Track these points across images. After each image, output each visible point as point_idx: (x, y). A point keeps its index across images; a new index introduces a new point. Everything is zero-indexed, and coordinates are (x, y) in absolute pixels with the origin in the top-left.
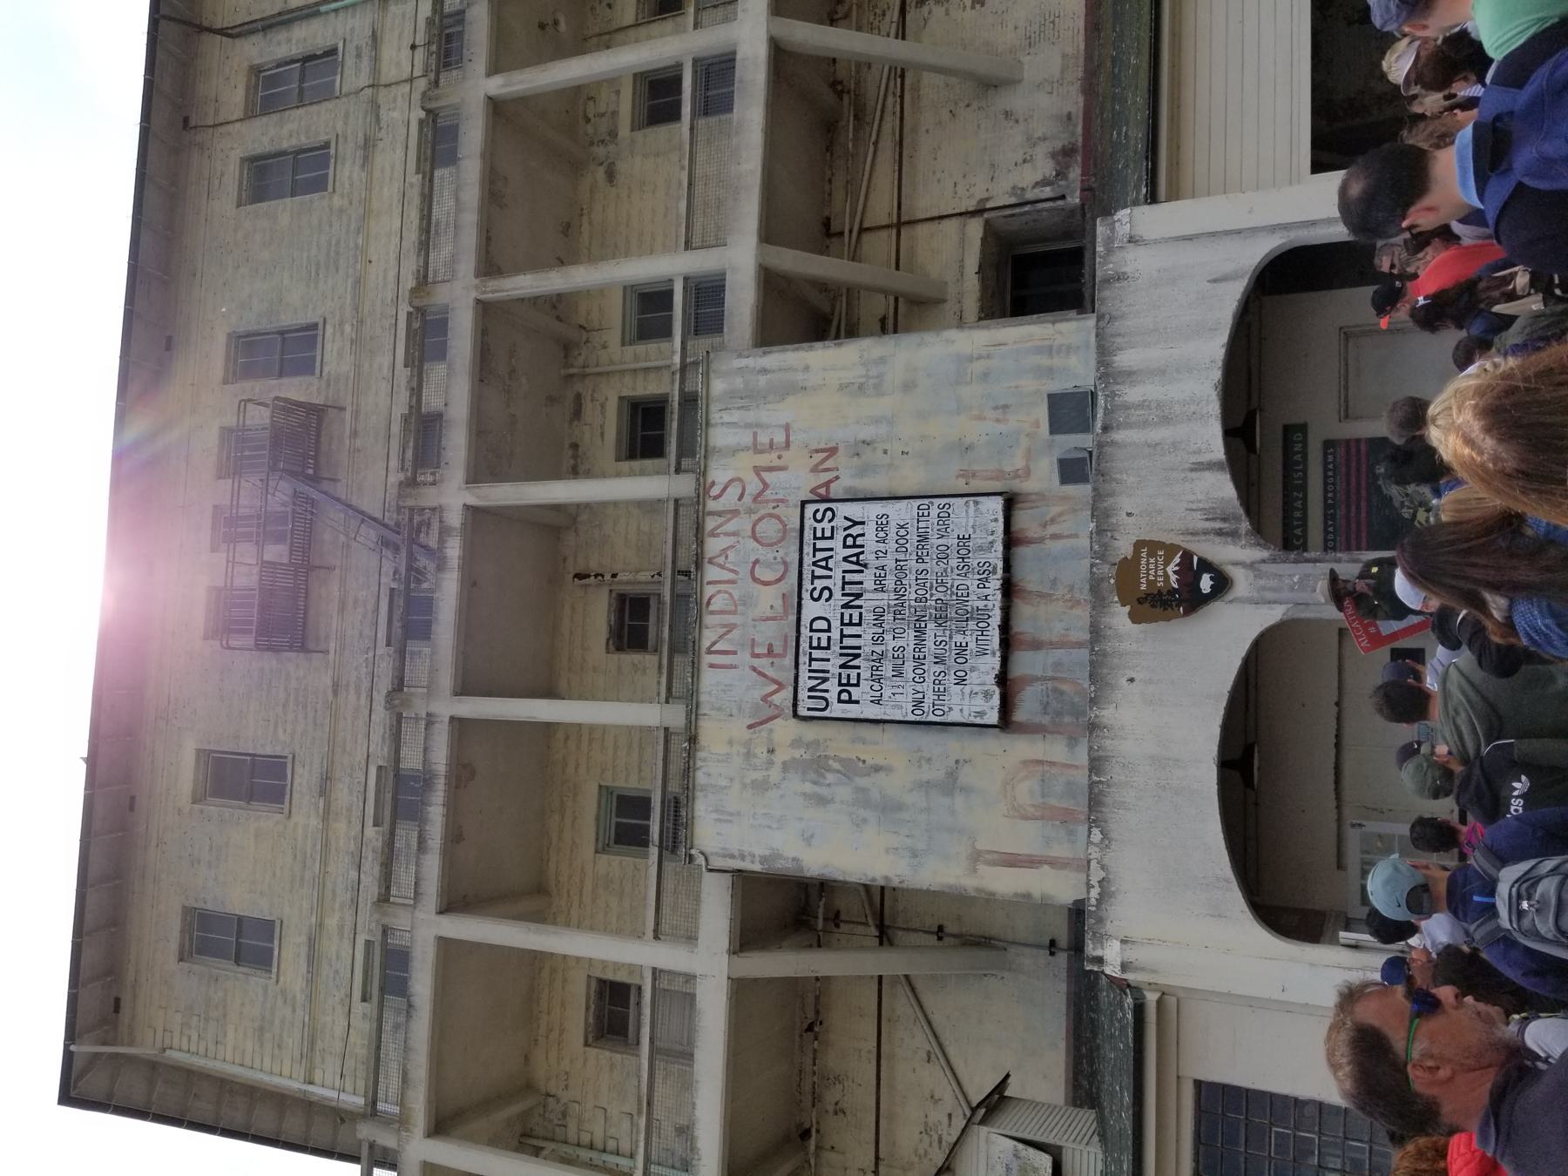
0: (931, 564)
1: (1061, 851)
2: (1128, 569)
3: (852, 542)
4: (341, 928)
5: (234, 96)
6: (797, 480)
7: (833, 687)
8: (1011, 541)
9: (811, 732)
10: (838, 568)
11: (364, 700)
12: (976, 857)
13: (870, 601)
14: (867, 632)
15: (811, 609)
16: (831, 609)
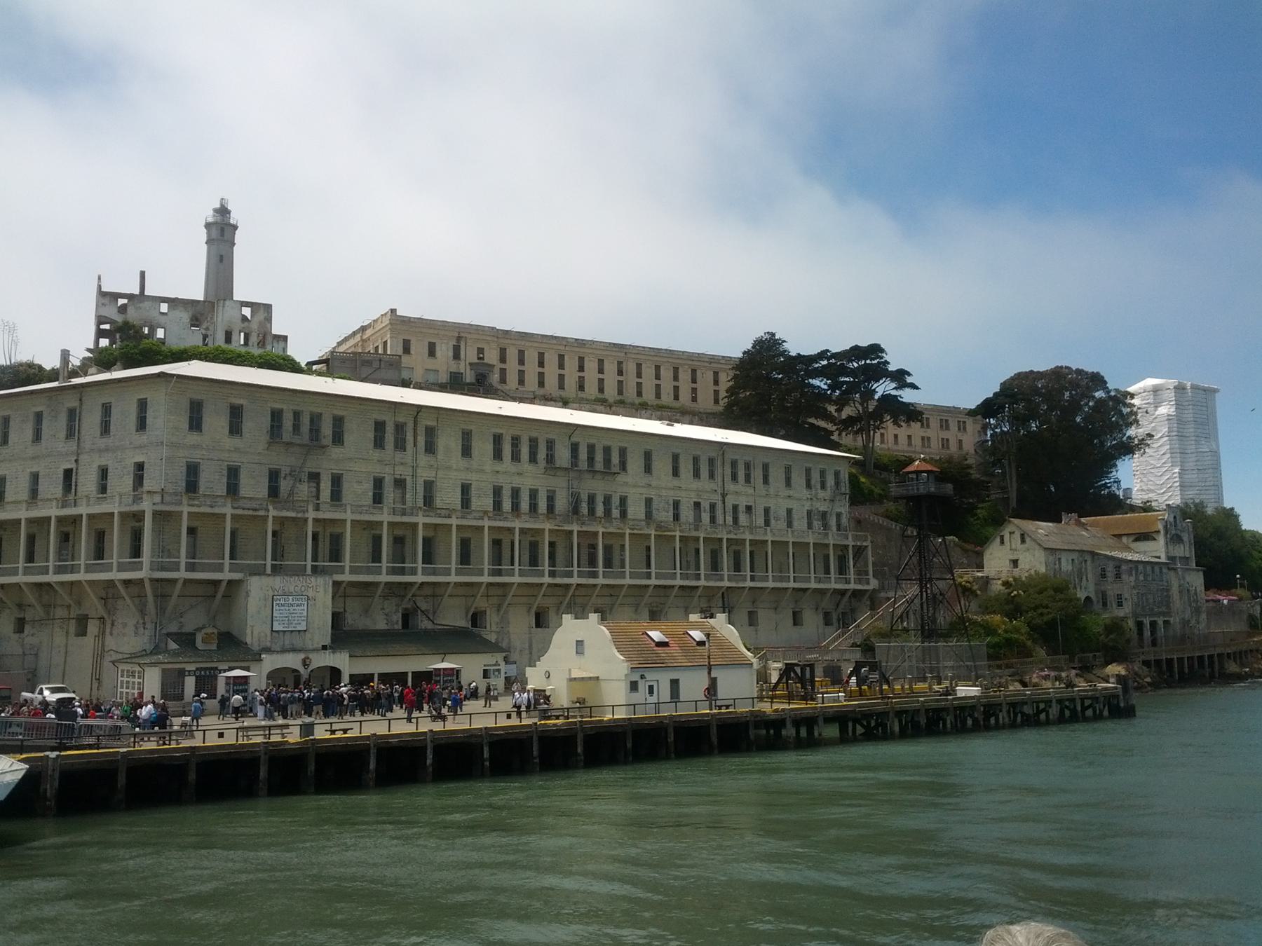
0: (296, 618)
1: (254, 640)
2: (308, 658)
3: (301, 605)
4: (203, 455)
5: (401, 419)
6: (311, 593)
7: (278, 602)
8: (299, 631)
9: (271, 599)
10: (297, 602)
11: (256, 461)
12: (252, 627)
13: (291, 608)
14: (287, 608)
15: (290, 597)
16: (290, 602)
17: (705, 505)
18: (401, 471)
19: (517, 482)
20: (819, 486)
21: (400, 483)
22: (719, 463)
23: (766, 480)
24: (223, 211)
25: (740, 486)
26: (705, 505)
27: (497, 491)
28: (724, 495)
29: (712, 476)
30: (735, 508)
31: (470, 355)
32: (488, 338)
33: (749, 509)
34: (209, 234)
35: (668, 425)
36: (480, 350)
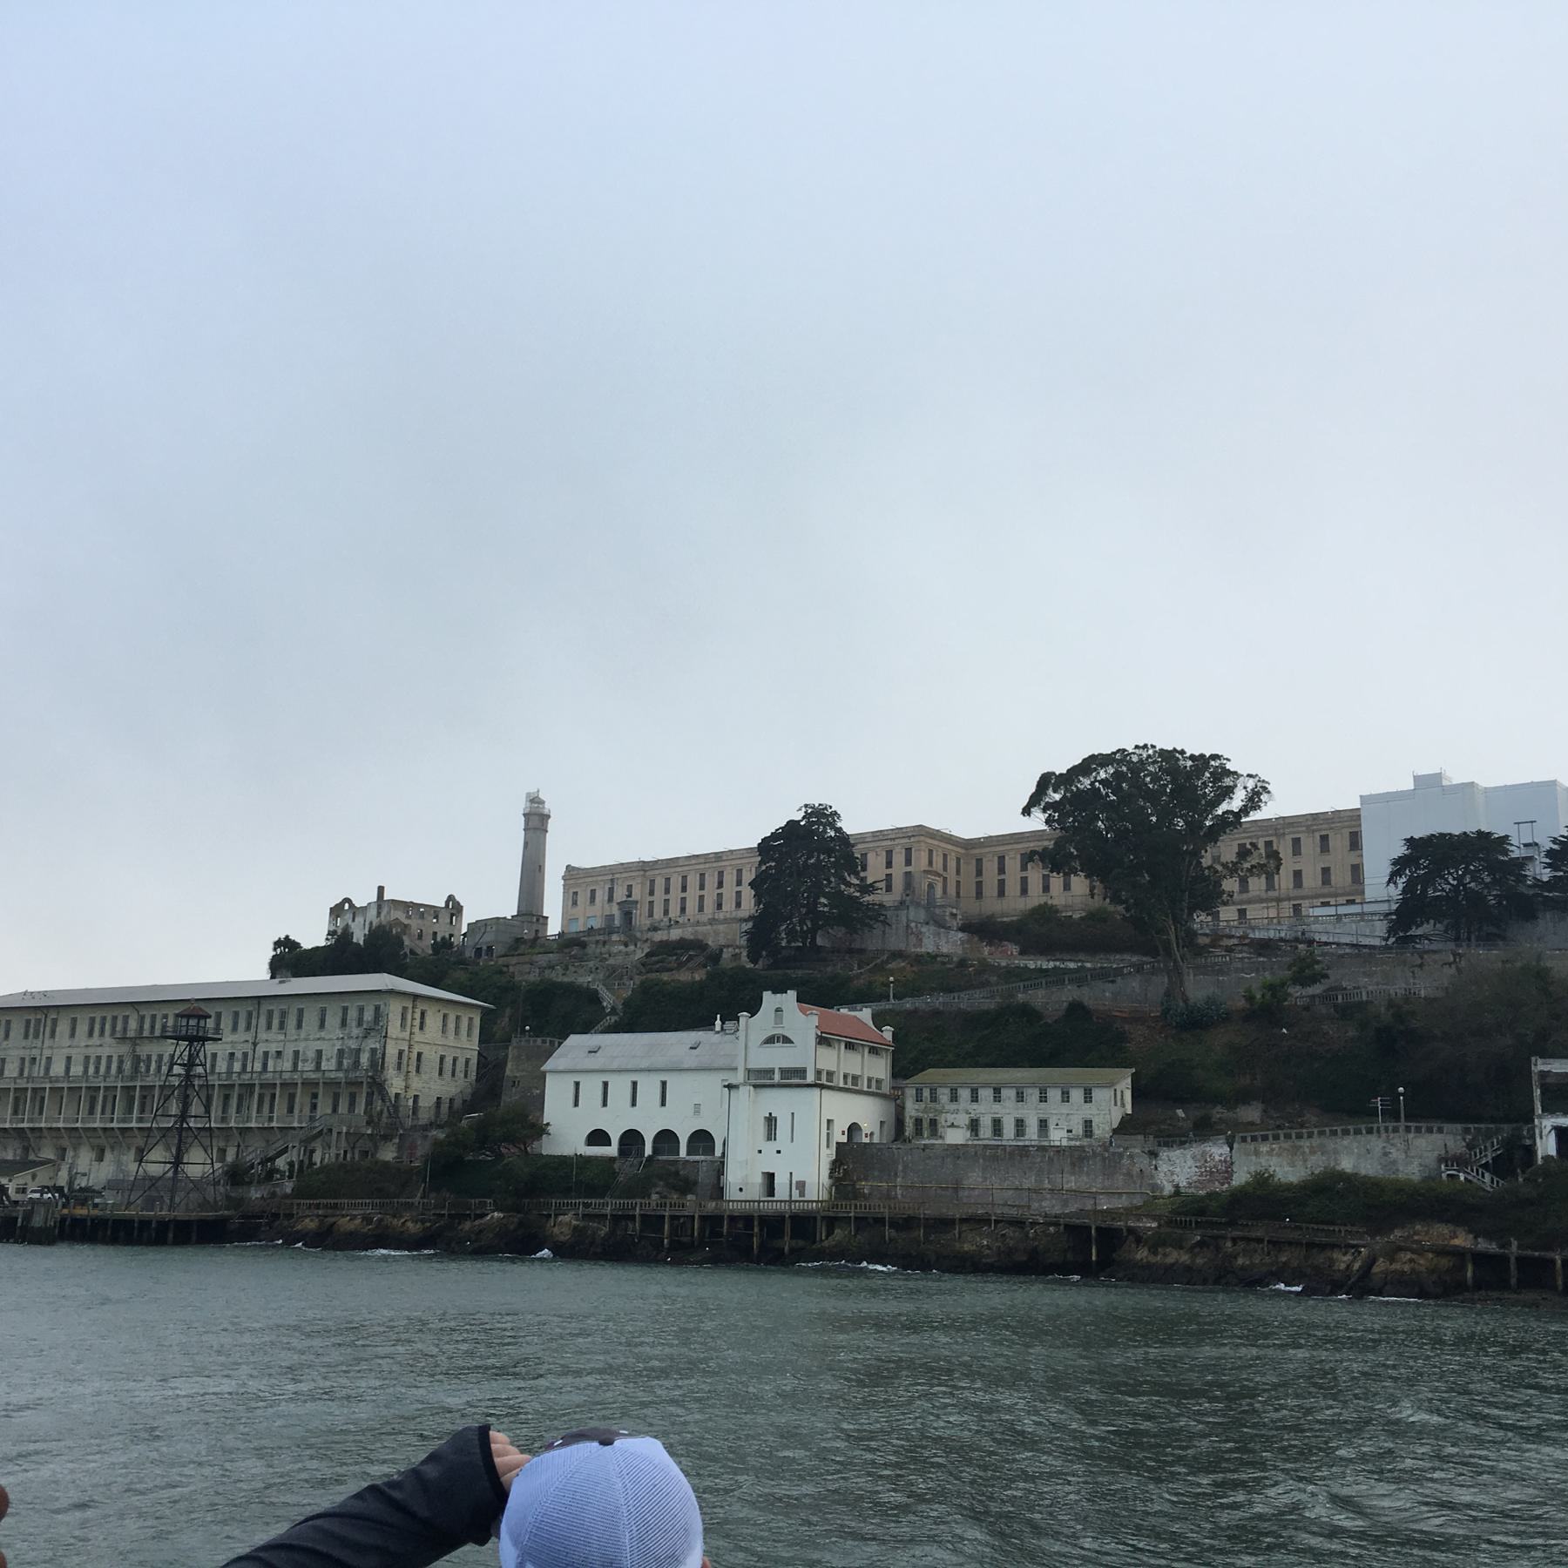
5: (38, 1017)
17: (239, 1055)
18: (35, 1052)
19: (99, 1051)
20: (354, 1024)
21: (34, 1060)
22: (255, 1014)
23: (299, 1026)
24: (535, 800)
25: (275, 1035)
26: (239, 1055)
27: (87, 1058)
28: (255, 1044)
29: (248, 1028)
30: (266, 1054)
31: (620, 895)
32: (633, 874)
33: (279, 1054)
34: (527, 823)
35: (281, 982)
36: (630, 887)
